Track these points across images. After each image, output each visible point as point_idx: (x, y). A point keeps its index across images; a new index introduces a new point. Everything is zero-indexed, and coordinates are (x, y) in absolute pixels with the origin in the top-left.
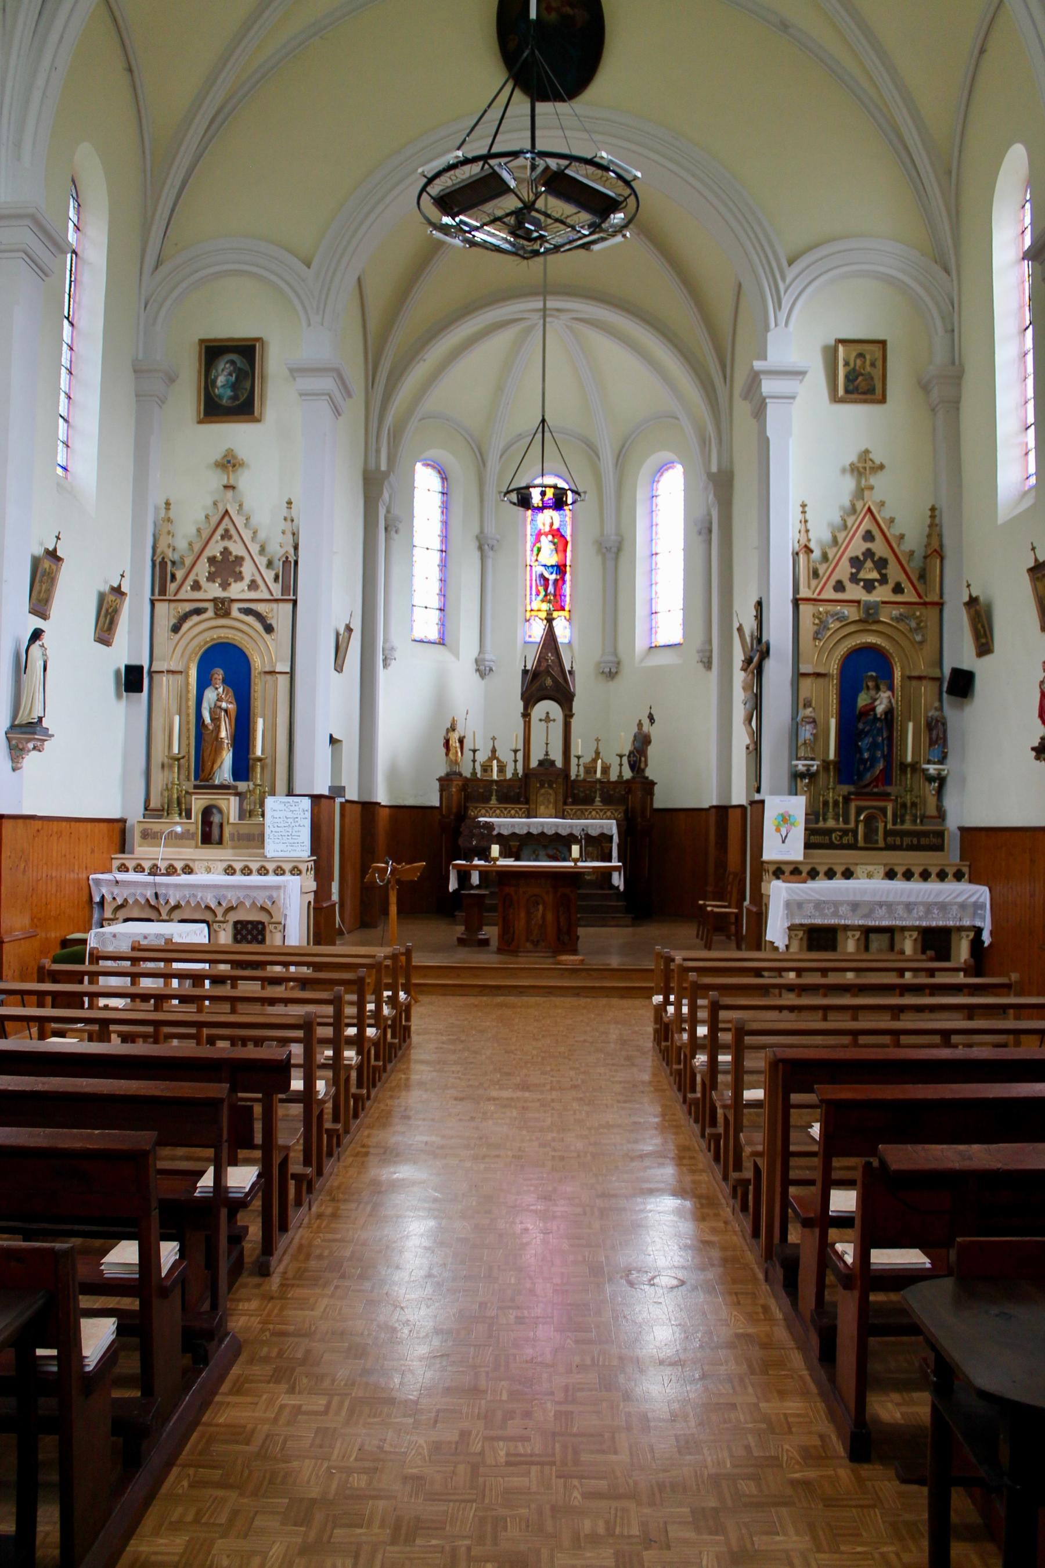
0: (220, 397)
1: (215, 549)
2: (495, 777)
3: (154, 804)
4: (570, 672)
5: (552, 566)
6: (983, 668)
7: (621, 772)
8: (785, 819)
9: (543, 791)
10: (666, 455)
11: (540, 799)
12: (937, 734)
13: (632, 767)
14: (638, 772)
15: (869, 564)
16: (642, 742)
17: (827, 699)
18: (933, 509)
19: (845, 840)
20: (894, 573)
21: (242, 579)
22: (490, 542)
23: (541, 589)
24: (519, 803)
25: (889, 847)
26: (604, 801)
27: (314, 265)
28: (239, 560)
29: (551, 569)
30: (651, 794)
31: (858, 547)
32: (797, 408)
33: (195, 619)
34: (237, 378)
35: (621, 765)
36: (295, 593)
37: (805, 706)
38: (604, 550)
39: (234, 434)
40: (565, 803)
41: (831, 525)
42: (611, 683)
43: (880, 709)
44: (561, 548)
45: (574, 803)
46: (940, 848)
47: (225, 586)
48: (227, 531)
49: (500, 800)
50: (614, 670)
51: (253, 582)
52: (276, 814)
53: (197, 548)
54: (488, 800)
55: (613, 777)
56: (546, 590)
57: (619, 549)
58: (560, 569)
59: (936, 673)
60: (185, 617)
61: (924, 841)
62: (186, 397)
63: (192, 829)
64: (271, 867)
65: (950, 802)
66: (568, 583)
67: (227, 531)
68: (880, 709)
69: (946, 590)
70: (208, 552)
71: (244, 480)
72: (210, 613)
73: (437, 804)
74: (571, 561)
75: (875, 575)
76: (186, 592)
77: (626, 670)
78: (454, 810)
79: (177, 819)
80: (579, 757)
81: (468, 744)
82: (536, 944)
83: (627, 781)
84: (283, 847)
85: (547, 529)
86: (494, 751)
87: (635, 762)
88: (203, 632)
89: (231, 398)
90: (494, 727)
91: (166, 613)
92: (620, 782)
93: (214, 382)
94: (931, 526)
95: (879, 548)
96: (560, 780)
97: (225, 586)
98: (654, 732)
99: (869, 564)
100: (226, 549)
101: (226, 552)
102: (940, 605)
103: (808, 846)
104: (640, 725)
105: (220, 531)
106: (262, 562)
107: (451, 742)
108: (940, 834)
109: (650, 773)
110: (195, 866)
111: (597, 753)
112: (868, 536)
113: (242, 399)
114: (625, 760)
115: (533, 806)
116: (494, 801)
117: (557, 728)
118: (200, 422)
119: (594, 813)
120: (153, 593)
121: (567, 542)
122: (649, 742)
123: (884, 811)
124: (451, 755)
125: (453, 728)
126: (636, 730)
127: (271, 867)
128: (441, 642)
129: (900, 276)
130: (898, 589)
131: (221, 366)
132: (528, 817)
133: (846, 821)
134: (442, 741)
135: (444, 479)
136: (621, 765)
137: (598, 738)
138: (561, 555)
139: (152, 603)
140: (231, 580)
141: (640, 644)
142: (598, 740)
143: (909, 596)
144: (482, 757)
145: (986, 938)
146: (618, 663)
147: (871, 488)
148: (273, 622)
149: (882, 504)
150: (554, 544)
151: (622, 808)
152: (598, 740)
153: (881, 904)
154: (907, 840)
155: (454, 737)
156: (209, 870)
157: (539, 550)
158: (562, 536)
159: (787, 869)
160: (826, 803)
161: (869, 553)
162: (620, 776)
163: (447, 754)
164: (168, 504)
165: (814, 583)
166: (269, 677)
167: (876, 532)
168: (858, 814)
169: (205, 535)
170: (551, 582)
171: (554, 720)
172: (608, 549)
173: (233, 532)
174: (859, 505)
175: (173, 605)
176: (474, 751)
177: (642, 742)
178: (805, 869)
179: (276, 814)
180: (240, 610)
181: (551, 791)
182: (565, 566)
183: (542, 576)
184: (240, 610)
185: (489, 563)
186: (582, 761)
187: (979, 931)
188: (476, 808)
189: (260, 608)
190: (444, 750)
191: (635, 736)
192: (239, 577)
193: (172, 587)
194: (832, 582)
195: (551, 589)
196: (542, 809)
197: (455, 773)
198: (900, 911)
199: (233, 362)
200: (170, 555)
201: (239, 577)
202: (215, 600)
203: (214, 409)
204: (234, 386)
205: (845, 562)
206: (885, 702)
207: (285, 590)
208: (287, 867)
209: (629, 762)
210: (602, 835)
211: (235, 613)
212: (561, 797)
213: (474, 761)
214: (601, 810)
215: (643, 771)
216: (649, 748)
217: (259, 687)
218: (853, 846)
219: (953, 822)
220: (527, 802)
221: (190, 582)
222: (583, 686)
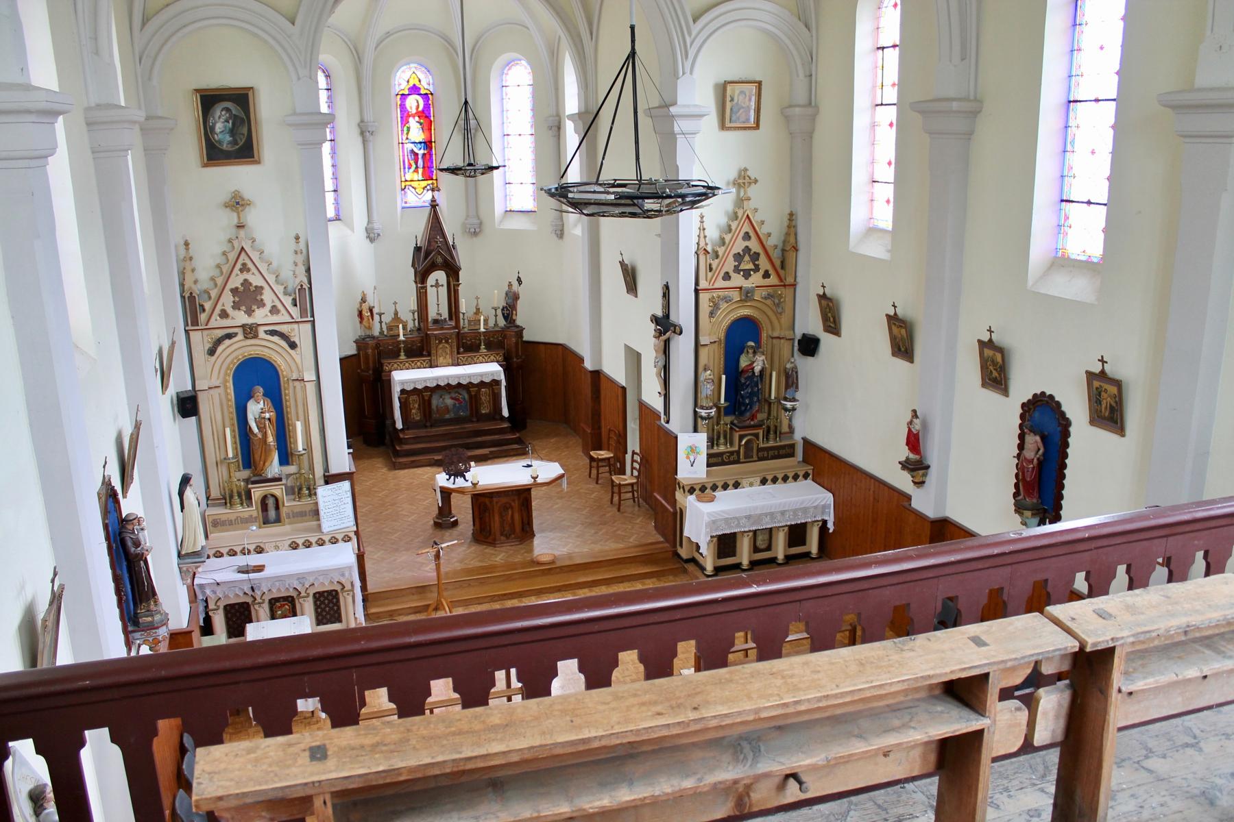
0: (220, 142)
1: (236, 281)
3: (215, 493)
6: (826, 339)
8: (693, 449)
10: (515, 55)
12: (791, 380)
13: (506, 318)
15: (747, 258)
16: (512, 300)
17: (713, 357)
18: (791, 214)
19: (732, 459)
20: (763, 263)
21: (264, 305)
23: (412, 162)
24: (422, 355)
25: (760, 459)
26: (489, 347)
27: (298, 21)
28: (259, 289)
31: (739, 246)
32: (698, 141)
33: (227, 342)
34: (234, 124)
36: (313, 316)
37: (705, 370)
39: (237, 176)
41: (718, 226)
43: (757, 369)
46: (792, 455)
47: (250, 312)
48: (244, 265)
51: (274, 307)
52: (326, 499)
53: (220, 281)
56: (416, 163)
58: (428, 144)
59: (788, 334)
60: (219, 342)
61: (782, 452)
62: (188, 144)
63: (255, 514)
64: (326, 538)
65: (797, 423)
67: (244, 265)
68: (757, 369)
69: (799, 274)
70: (231, 285)
71: (252, 217)
72: (240, 336)
75: (751, 266)
76: (216, 321)
78: (371, 365)
79: (240, 508)
81: (375, 311)
82: (508, 537)
84: (334, 523)
85: (414, 111)
86: (396, 313)
88: (237, 350)
89: (230, 143)
91: (201, 341)
93: (212, 129)
94: (789, 227)
95: (754, 245)
97: (250, 312)
98: (521, 290)
99: (747, 258)
100: (246, 280)
101: (246, 283)
102: (794, 285)
103: (709, 465)
104: (510, 285)
105: (239, 266)
106: (279, 290)
108: (792, 446)
109: (520, 320)
110: (266, 547)
111: (478, 309)
112: (747, 237)
113: (241, 144)
114: (499, 312)
116: (403, 356)
117: (443, 291)
118: (205, 166)
120: (186, 324)
123: (757, 436)
125: (363, 300)
127: (326, 538)
128: (338, 218)
129: (776, 31)
130: (766, 275)
131: (218, 113)
133: (731, 444)
134: (356, 313)
135: (328, 76)
138: (427, 133)
139: (187, 332)
140: (254, 307)
141: (499, 209)
142: (477, 298)
143: (773, 280)
144: (387, 318)
145: (831, 526)
146: (481, 223)
147: (749, 199)
148: (296, 340)
149: (756, 210)
153: (766, 515)
154: (771, 453)
155: (365, 307)
156: (277, 548)
157: (409, 129)
159: (697, 488)
160: (719, 433)
161: (747, 250)
162: (496, 325)
164: (187, 244)
165: (710, 274)
166: (297, 383)
167: (752, 234)
168: (740, 441)
169: (226, 269)
173: (250, 265)
174: (740, 214)
175: (205, 332)
177: (512, 300)
178: (709, 486)
179: (326, 499)
180: (266, 332)
183: (412, 151)
184: (266, 332)
185: (371, 145)
187: (825, 522)
189: (283, 329)
190: (358, 320)
192: (261, 304)
193: (203, 317)
194: (722, 274)
195: (420, 162)
196: (441, 360)
197: (369, 337)
198: (779, 517)
199: (228, 110)
200: (196, 290)
201: (261, 304)
202: (243, 326)
203: (214, 154)
204: (232, 132)
205: (731, 258)
206: (761, 364)
207: (303, 313)
208: (340, 537)
210: (494, 381)
211: (262, 334)
213: (381, 322)
217: (290, 395)
218: (737, 462)
219: (798, 437)
220: (429, 355)
221: (217, 311)
222: (463, 257)
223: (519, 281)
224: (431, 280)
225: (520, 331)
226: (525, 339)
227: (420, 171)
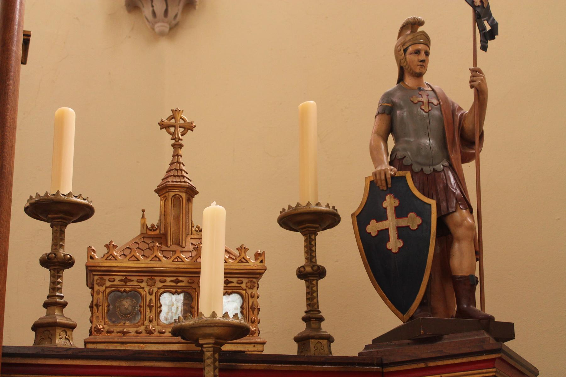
7: (313, 317)
13: (390, 272)
35: (312, 274)
80: (58, 212)
104: (413, 41)
114: (340, 248)
136: (312, 274)
142: (176, 127)
209: (373, 250)
216: (480, 154)
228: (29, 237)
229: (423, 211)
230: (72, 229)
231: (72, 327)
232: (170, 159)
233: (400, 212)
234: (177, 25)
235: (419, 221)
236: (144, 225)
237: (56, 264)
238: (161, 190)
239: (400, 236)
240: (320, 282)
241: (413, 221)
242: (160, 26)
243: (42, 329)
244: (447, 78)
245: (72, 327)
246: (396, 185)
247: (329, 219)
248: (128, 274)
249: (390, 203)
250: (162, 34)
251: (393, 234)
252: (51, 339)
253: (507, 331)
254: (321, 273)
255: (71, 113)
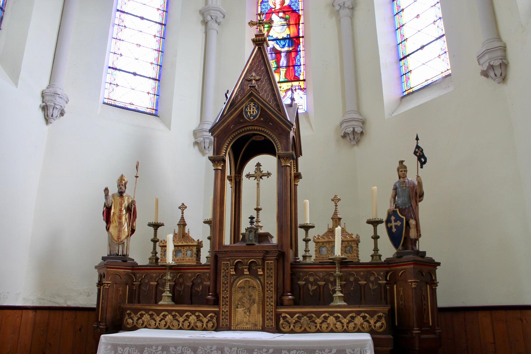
2: (170, 260)
4: (290, 106)
5: (284, 39)
7: (376, 249)
9: (240, 282)
11: (237, 296)
13: (394, 238)
14: (405, 246)
16: (408, 199)
22: (213, 13)
24: (207, 303)
26: (355, 296)
29: (282, 43)
30: (433, 283)
35: (376, 237)
38: (337, 8)
40: (280, 303)
42: (356, 148)
44: (292, 22)
45: (296, 303)
49: (176, 299)
50: (358, 130)
54: (157, 298)
55: (365, 255)
56: (278, 62)
57: (353, 9)
58: (294, 41)
66: (302, 53)
73: (95, 306)
74: (303, 32)
77: (374, 130)
80: (307, 228)
83: (388, 262)
85: (278, 7)
87: (398, 228)
90: (183, 187)
92: (376, 264)
96: (271, 262)
98: (428, 177)
107: (118, 209)
115: (225, 309)
116: (166, 300)
117: (270, 186)
119: (331, 320)
121: (299, 16)
122: (420, 196)
124: (111, 230)
126: (395, 178)
128: (155, 114)
132: (217, 329)
134: (102, 209)
136: (376, 237)
137: (337, 199)
138: (293, 29)
141: (390, 92)
146: (363, 122)
150: (286, 19)
151: (382, 310)
152: (336, 200)
158: (294, 11)
163: (108, 229)
170: (283, 55)
171: (268, 175)
172: (342, 6)
176: (156, 226)
177: (408, 199)
181: (255, 283)
182: (298, 37)
183: (274, 49)
185: (213, 35)
186: (312, 233)
188: (136, 311)
191: (395, 189)
196: (240, 314)
212: (271, 294)
213: (155, 241)
214: (345, 314)
215: (415, 241)
220: (216, 302)
223: (421, 156)
224: (250, 167)
225: (427, 268)
226: (442, 303)
227: (283, 71)
228: (301, 233)
229: (401, 220)
230: (310, 231)
231: (311, 256)
232: (334, 209)
233: (395, 221)
234: (359, 141)
235: (400, 223)
236: (328, 228)
237: (307, 241)
238: (332, 219)
239: (395, 228)
240: (378, 240)
241: (399, 223)
242: (354, 142)
243: (305, 257)
244: (411, 177)
245: (311, 256)
246: (394, 212)
247: (381, 222)
248: (323, 243)
249: (393, 218)
250: (354, 145)
251: (393, 227)
252: (306, 259)
253: (424, 253)
254: (378, 237)
255: (307, 201)
